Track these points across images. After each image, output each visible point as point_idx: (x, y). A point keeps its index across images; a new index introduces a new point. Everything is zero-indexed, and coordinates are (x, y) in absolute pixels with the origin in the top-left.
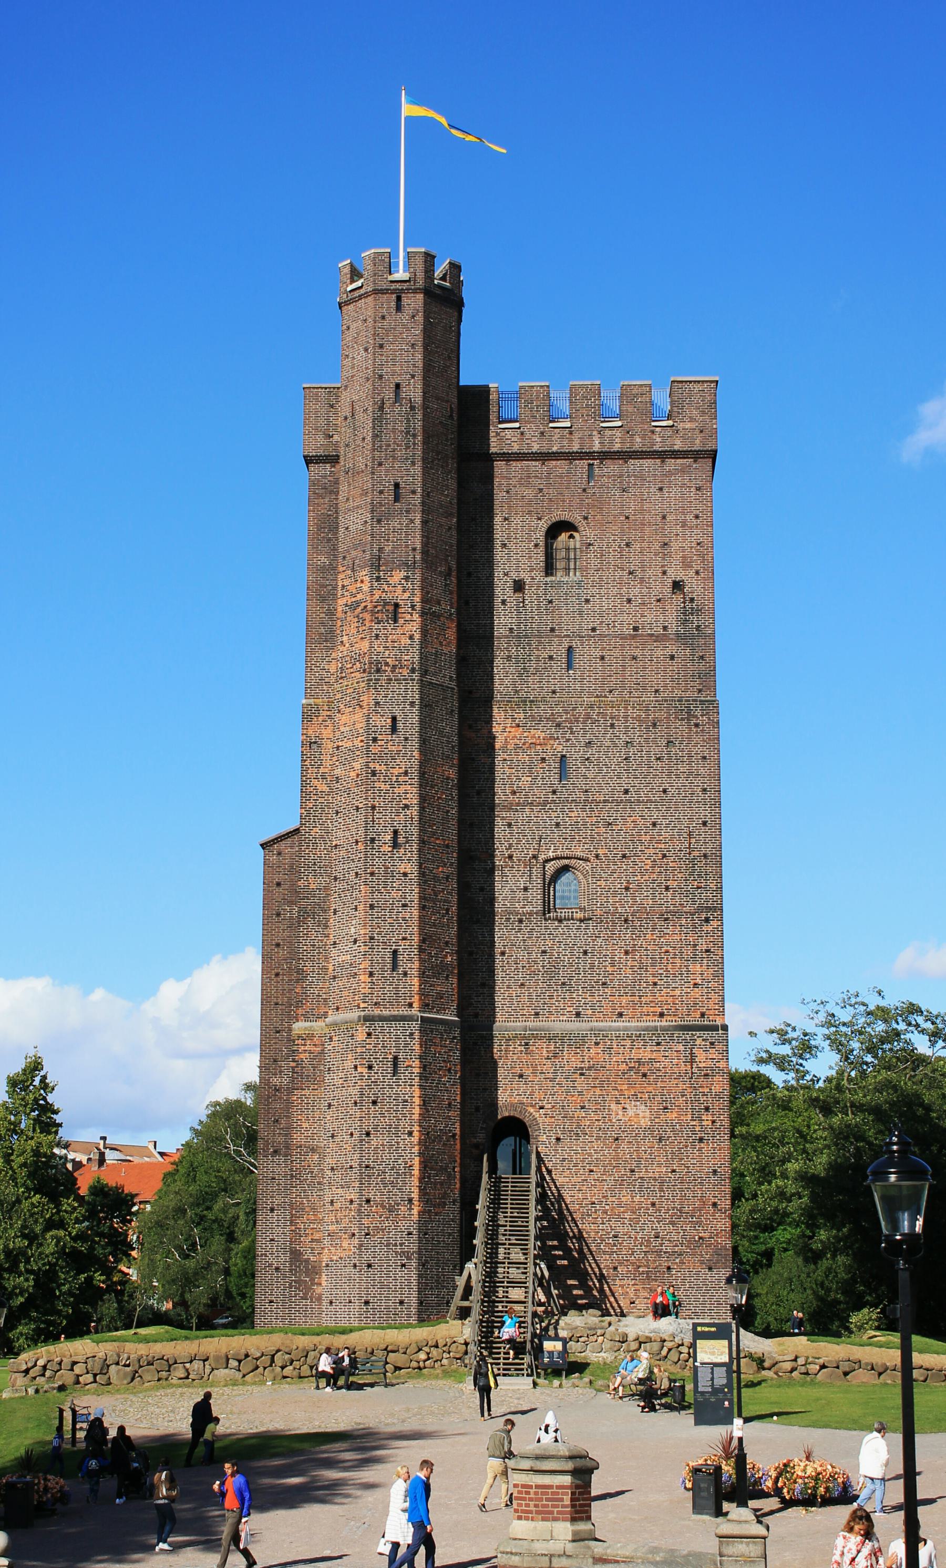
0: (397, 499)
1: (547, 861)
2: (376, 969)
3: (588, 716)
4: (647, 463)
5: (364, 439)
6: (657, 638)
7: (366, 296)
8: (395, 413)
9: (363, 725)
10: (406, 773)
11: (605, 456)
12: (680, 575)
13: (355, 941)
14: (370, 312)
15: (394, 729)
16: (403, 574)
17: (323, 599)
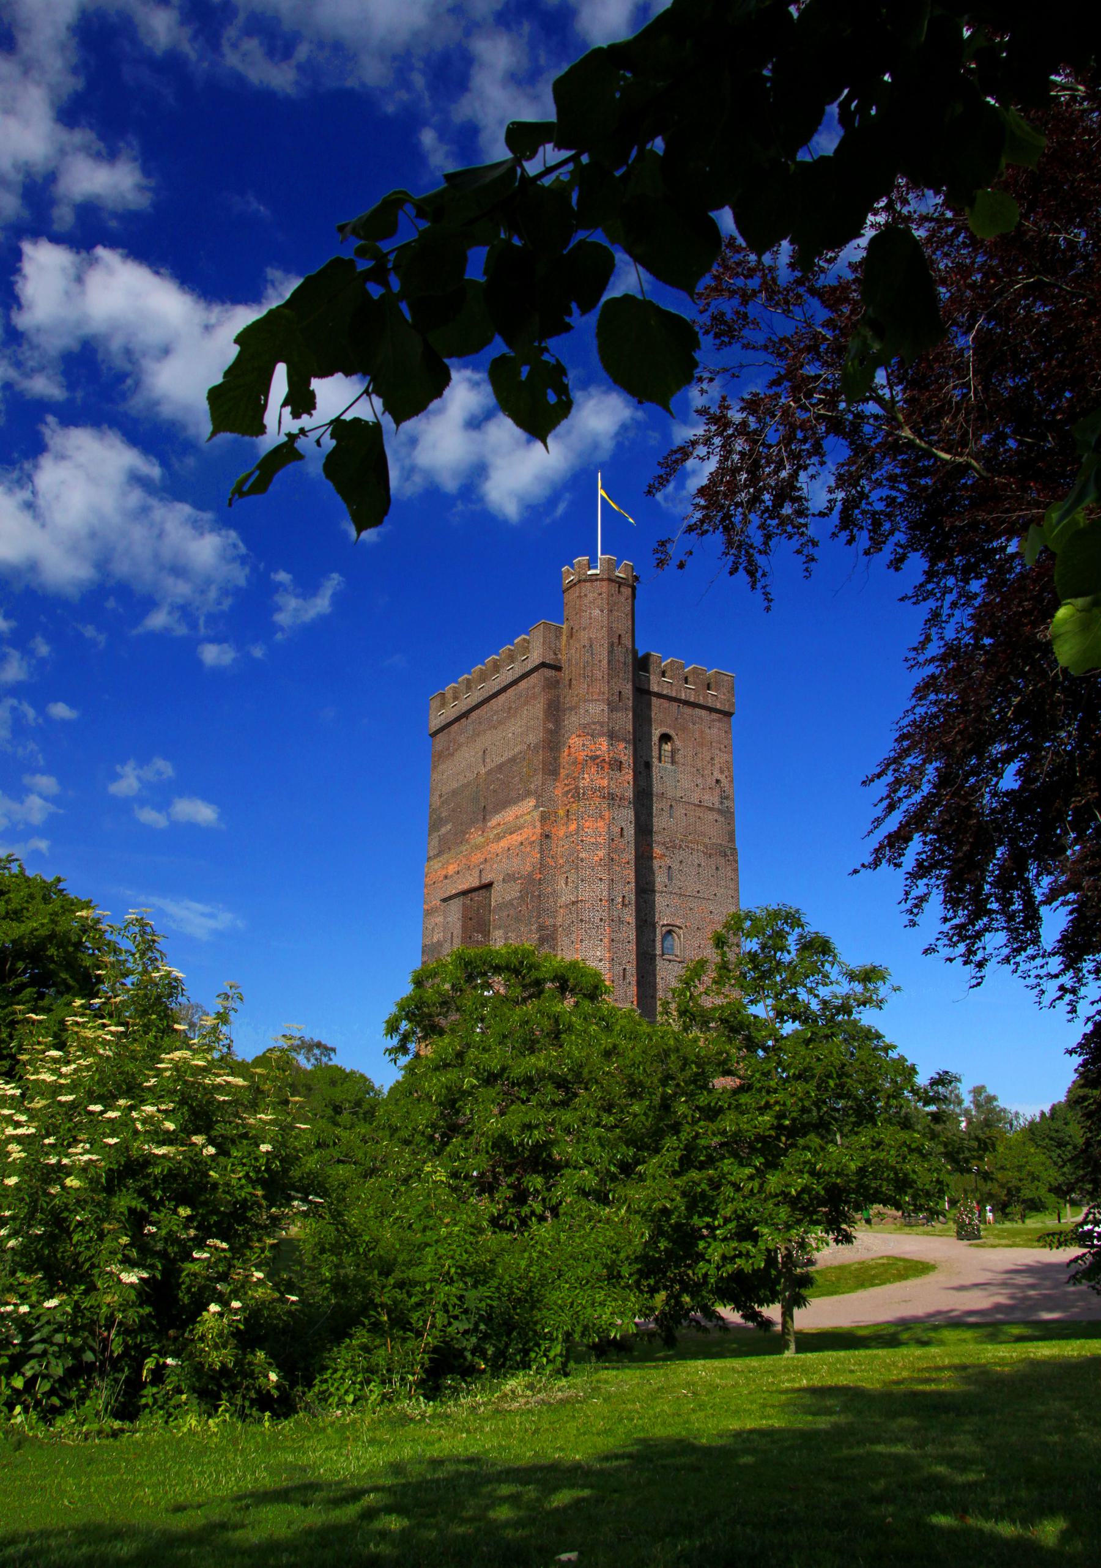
0: (620, 701)
1: (663, 926)
2: (616, 978)
3: (680, 847)
4: (703, 713)
5: (600, 661)
6: (710, 809)
7: (602, 580)
8: (619, 650)
9: (606, 829)
10: (628, 863)
11: (686, 703)
12: (719, 777)
13: (601, 960)
14: (604, 590)
15: (622, 835)
16: (624, 745)
17: (551, 749)
